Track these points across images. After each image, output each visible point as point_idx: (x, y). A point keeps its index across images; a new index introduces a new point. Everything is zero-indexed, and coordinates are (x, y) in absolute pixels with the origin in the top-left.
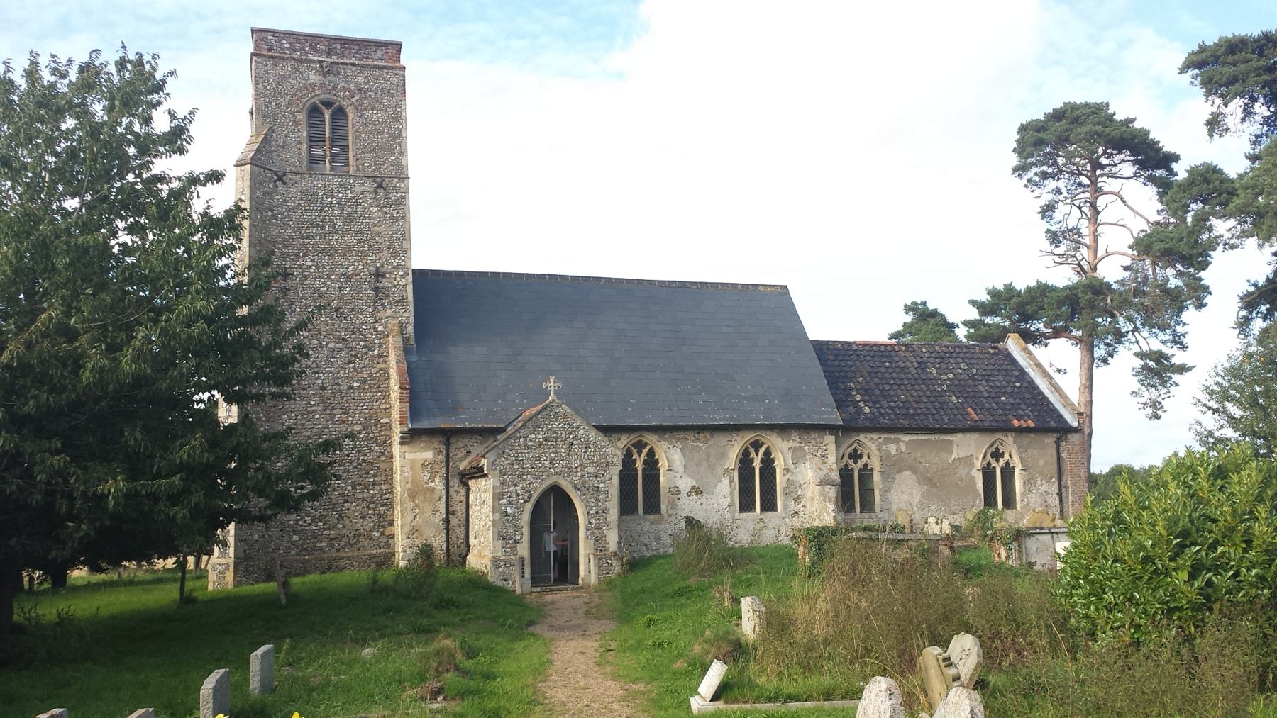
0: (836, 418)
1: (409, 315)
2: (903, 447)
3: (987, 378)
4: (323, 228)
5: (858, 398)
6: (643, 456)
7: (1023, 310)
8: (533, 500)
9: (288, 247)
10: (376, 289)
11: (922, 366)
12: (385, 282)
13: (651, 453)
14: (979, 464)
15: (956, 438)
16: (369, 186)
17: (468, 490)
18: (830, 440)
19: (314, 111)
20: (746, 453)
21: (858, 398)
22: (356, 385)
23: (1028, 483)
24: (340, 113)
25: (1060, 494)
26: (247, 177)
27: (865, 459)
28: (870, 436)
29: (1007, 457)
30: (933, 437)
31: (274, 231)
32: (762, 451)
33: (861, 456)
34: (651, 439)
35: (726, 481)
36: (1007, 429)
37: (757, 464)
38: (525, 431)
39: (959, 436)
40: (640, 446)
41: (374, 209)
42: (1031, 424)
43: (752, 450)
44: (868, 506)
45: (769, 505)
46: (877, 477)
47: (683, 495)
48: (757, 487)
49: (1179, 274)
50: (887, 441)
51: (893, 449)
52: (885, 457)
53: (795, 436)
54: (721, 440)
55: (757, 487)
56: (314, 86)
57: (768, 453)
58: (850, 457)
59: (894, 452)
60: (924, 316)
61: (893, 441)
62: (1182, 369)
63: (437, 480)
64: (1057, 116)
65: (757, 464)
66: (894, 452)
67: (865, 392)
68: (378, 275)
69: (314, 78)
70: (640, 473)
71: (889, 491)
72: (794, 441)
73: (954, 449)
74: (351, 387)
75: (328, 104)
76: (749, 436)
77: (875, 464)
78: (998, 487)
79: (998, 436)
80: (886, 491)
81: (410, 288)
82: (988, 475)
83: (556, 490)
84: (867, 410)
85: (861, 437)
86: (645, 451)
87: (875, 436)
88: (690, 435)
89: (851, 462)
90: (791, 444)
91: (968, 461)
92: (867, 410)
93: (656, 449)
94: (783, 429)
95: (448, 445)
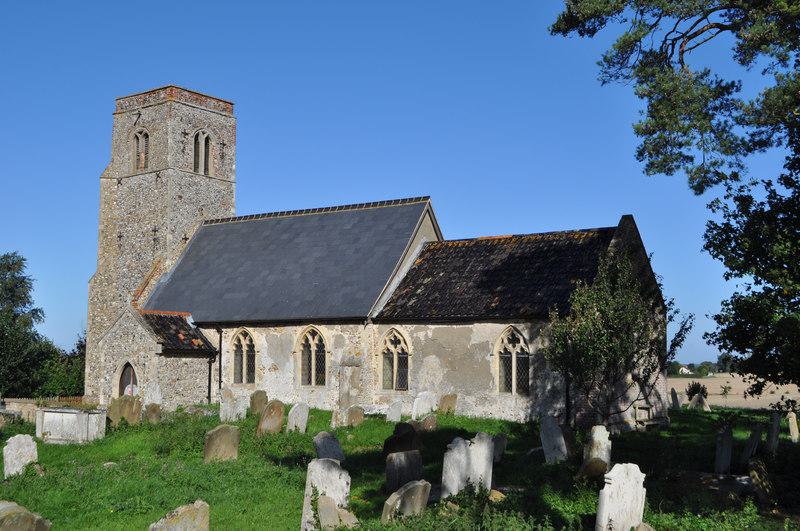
2: (430, 334)
4: (135, 207)
10: (154, 240)
13: (251, 340)
14: (497, 348)
15: (477, 327)
24: (146, 136)
31: (116, 213)
34: (250, 330)
35: (292, 359)
37: (314, 348)
38: (115, 328)
40: (245, 334)
43: (310, 337)
45: (321, 381)
50: (416, 330)
51: (421, 335)
52: (416, 342)
53: (338, 327)
54: (290, 329)
55: (316, 368)
57: (321, 340)
58: (392, 342)
71: (419, 368)
75: (141, 133)
77: (410, 350)
80: (415, 372)
83: (128, 365)
90: (334, 332)
91: (484, 347)
94: (329, 321)
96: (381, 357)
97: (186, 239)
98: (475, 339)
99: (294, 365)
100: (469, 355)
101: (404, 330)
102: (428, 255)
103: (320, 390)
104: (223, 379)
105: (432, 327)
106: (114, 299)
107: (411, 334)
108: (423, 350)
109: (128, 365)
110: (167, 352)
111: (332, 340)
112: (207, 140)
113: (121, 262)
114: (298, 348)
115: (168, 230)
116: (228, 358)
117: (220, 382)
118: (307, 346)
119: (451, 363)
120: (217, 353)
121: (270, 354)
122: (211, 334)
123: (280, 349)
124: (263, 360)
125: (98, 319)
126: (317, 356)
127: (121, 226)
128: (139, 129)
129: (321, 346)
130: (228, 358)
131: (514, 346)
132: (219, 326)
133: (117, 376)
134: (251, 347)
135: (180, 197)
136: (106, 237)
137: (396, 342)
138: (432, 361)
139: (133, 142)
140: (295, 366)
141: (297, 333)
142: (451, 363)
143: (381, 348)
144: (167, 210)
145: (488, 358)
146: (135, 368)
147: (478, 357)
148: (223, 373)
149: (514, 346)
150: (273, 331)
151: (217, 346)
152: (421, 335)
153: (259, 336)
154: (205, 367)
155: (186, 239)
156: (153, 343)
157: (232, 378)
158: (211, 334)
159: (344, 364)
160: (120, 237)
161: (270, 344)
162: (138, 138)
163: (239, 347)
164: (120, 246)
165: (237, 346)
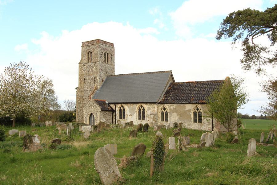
2: (174, 107)
12: (96, 79)
13: (124, 108)
15: (187, 105)
19: (88, 53)
24: (91, 53)
25: (213, 120)
27: (166, 110)
28: (167, 105)
29: (200, 110)
30: (181, 105)
31: (83, 73)
33: (166, 109)
34: (123, 105)
36: (199, 103)
37: (142, 110)
38: (88, 104)
39: (187, 104)
40: (122, 106)
43: (141, 107)
44: (167, 120)
47: (128, 116)
50: (171, 106)
51: (172, 107)
52: (170, 109)
54: (135, 105)
57: (144, 108)
58: (163, 109)
59: (172, 108)
66: (172, 108)
68: (95, 78)
70: (122, 111)
72: (148, 105)
73: (186, 108)
75: (90, 52)
77: (168, 111)
79: (197, 105)
80: (170, 117)
82: (195, 114)
83: (92, 114)
85: (165, 104)
87: (168, 105)
89: (163, 110)
90: (148, 106)
91: (189, 111)
94: (146, 103)
96: (160, 113)
97: (103, 80)
99: (136, 115)
100: (185, 113)
101: (167, 106)
102: (172, 86)
104: (116, 118)
105: (175, 105)
106: (83, 96)
107: (169, 107)
108: (172, 111)
109: (92, 114)
110: (102, 110)
111: (147, 109)
112: (108, 54)
113: (85, 86)
115: (98, 78)
116: (117, 113)
117: (116, 119)
118: (140, 110)
119: (180, 115)
120: (115, 111)
121: (129, 112)
122: (113, 106)
123: (132, 111)
124: (127, 113)
125: (79, 101)
128: (89, 51)
129: (144, 110)
130: (117, 113)
131: (198, 111)
132: (115, 104)
133: (88, 117)
134: (124, 110)
135: (101, 69)
136: (81, 79)
137: (164, 109)
138: (175, 114)
139: (87, 54)
140: (137, 115)
141: (137, 106)
143: (160, 111)
144: (98, 73)
145: (191, 113)
146: (94, 115)
147: (188, 113)
148: (116, 116)
149: (198, 111)
150: (131, 106)
151: (114, 109)
153: (126, 107)
154: (111, 115)
155: (103, 80)
156: (99, 108)
157: (119, 118)
158: (113, 106)
159: (151, 115)
160: (85, 79)
161: (129, 109)
162: (89, 53)
163: (120, 110)
164: (85, 82)
165: (119, 109)
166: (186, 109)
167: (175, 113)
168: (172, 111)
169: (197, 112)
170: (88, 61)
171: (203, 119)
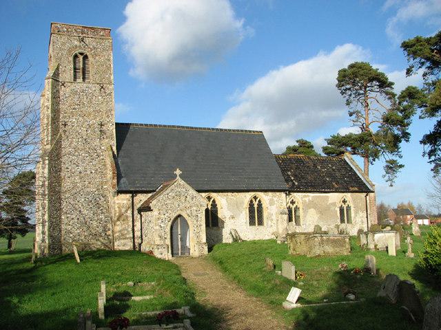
0: (287, 186)
1: (114, 142)
3: (339, 170)
5: (293, 178)
6: (211, 203)
7: (339, 144)
8: (171, 221)
9: (65, 113)
10: (101, 131)
11: (315, 166)
12: (104, 128)
16: (98, 87)
17: (141, 216)
18: (283, 195)
19: (76, 57)
20: (251, 201)
21: (293, 178)
22: (93, 171)
23: (356, 213)
24: (86, 57)
25: (367, 217)
26: (50, 84)
28: (298, 194)
32: (257, 200)
33: (294, 203)
34: (214, 195)
37: (256, 206)
41: (100, 98)
42: (356, 189)
43: (254, 200)
44: (298, 223)
45: (261, 223)
46: (352, 209)
48: (256, 215)
49: (398, 129)
51: (307, 199)
52: (304, 203)
53: (270, 194)
55: (256, 215)
56: (76, 46)
57: (260, 201)
60: (305, 146)
61: (305, 196)
62: (401, 166)
63: (129, 212)
64: (352, 66)
65: (256, 206)
67: (295, 176)
69: (76, 43)
74: (91, 173)
75: (81, 54)
76: (253, 194)
77: (300, 206)
78: (344, 214)
79: (345, 194)
81: (114, 130)
82: (342, 210)
84: (297, 184)
85: (295, 194)
86: (211, 200)
88: (230, 194)
89: (291, 205)
90: (269, 197)
91: (334, 204)
92: (297, 184)
93: (216, 200)
95: (133, 197)
98: (330, 201)
99: (244, 216)
101: (298, 197)
103: (261, 227)
108: (308, 206)
111: (268, 202)
114: (246, 205)
118: (251, 205)
119: (321, 212)
126: (258, 210)
127: (65, 117)
137: (293, 202)
138: (312, 211)
142: (321, 212)
152: (307, 199)
166: (329, 202)
167: (312, 209)
168: (308, 206)
169: (345, 206)
170: (75, 78)
171: (355, 218)
